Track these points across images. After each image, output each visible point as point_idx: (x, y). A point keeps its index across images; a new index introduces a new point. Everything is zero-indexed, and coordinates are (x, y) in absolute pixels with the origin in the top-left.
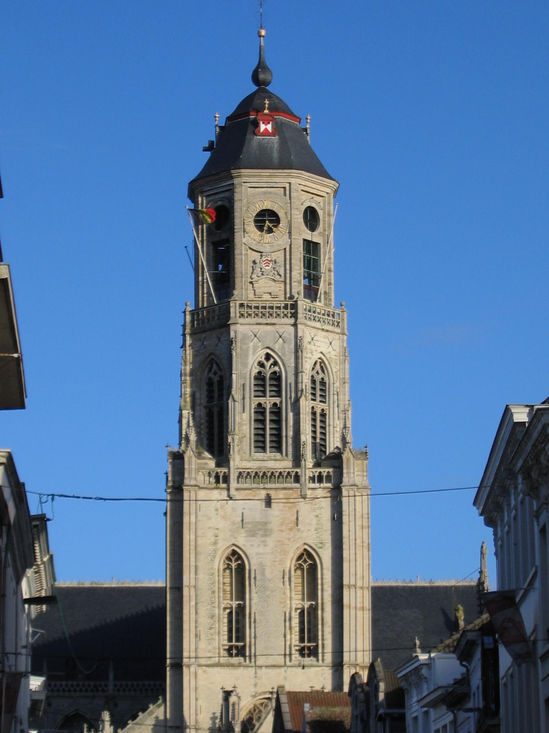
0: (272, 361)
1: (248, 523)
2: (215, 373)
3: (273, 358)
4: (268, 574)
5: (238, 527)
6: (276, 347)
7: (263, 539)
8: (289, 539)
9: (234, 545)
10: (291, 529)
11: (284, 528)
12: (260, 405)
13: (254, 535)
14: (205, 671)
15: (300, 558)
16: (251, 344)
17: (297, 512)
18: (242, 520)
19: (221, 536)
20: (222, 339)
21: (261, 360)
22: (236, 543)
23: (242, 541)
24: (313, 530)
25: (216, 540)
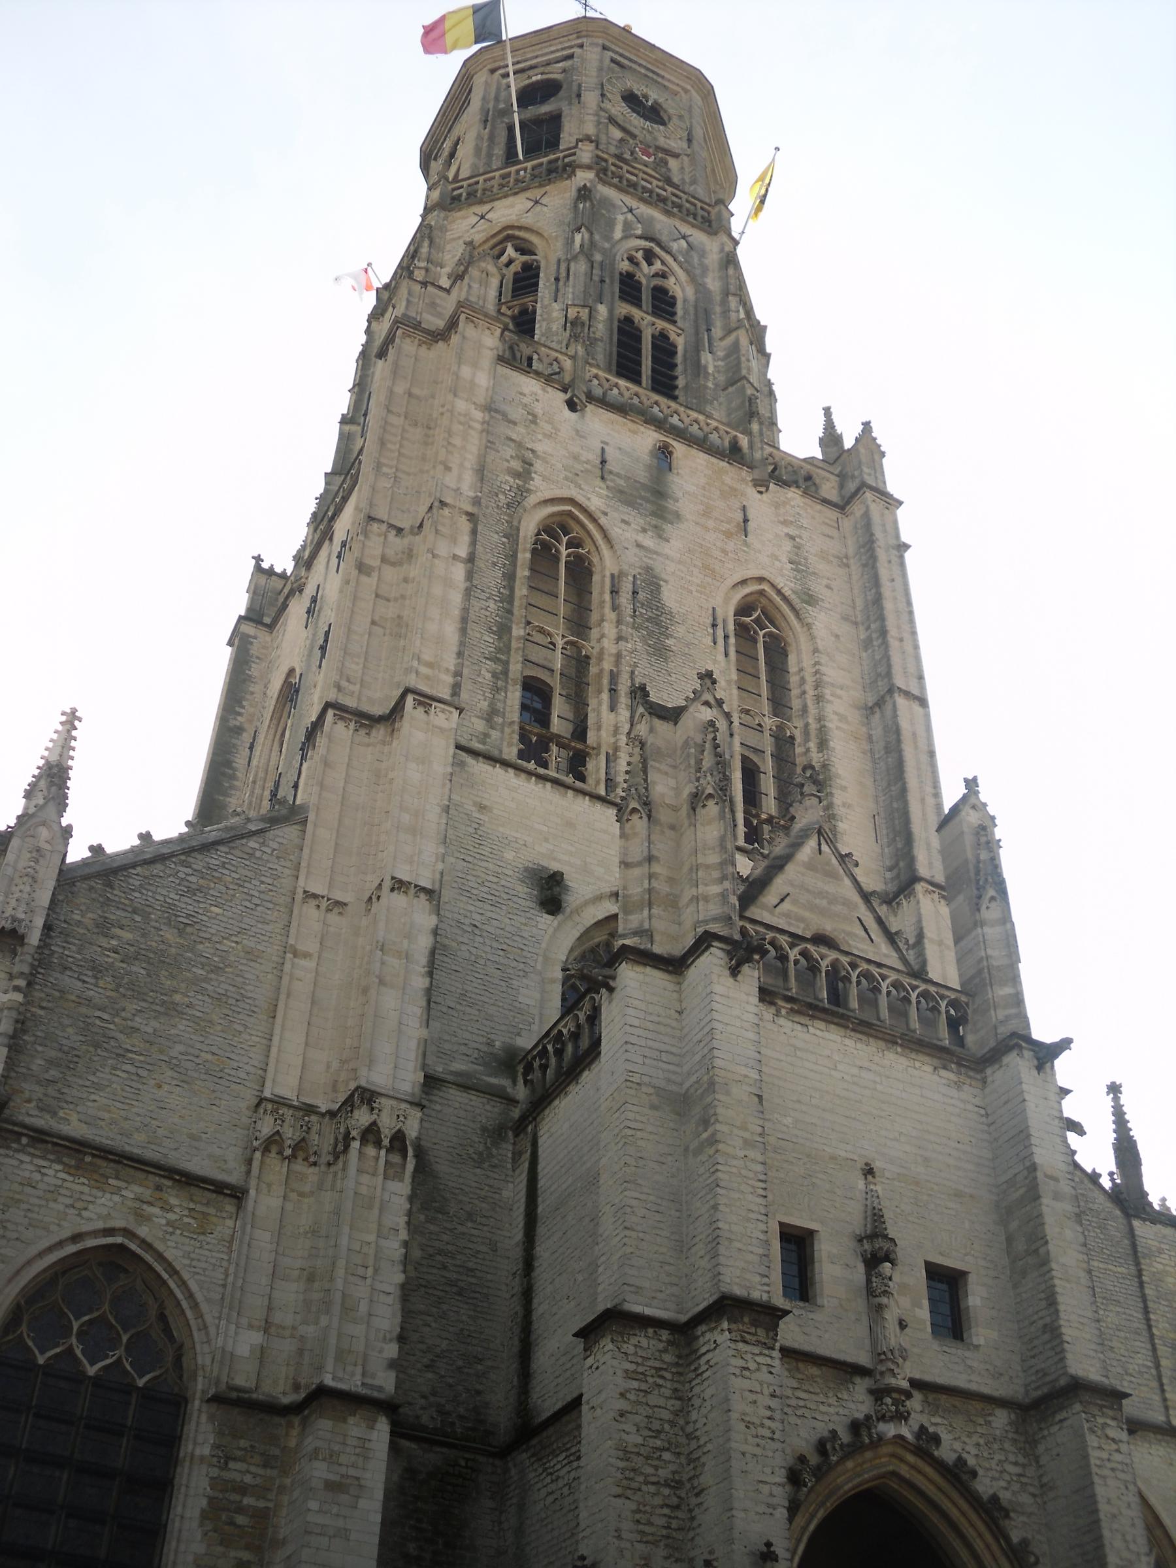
0: (658, 265)
1: (618, 475)
2: (510, 262)
3: (663, 263)
4: (670, 597)
5: (587, 471)
6: (675, 246)
7: (654, 521)
8: (724, 551)
9: (571, 501)
10: (729, 535)
11: (711, 524)
12: (628, 320)
13: (630, 503)
14: (462, 764)
15: (744, 609)
16: (620, 218)
17: (744, 508)
18: (603, 462)
19: (538, 466)
20: (544, 201)
21: (634, 253)
22: (580, 499)
23: (595, 498)
24: (785, 559)
25: (529, 473)
